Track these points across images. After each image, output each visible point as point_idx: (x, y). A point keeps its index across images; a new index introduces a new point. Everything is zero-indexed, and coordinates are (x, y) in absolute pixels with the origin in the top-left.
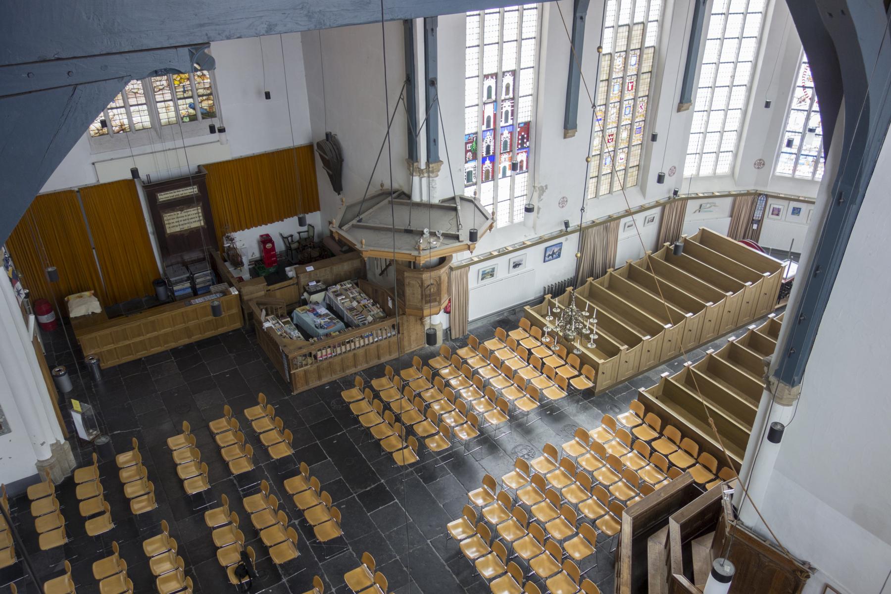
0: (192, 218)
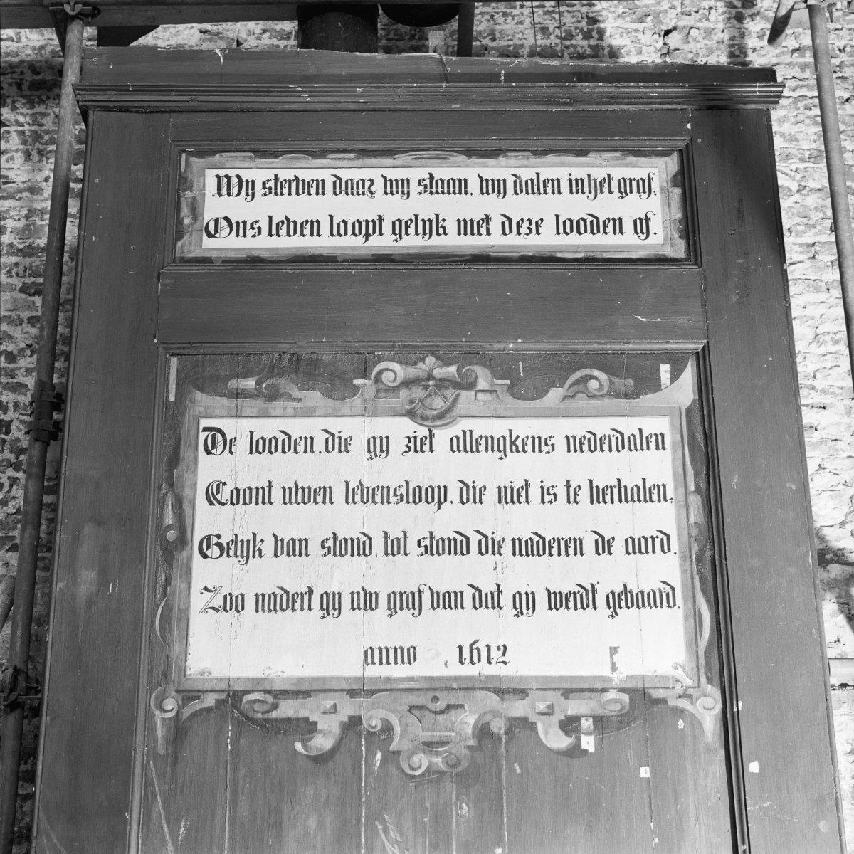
0: (535, 547)
